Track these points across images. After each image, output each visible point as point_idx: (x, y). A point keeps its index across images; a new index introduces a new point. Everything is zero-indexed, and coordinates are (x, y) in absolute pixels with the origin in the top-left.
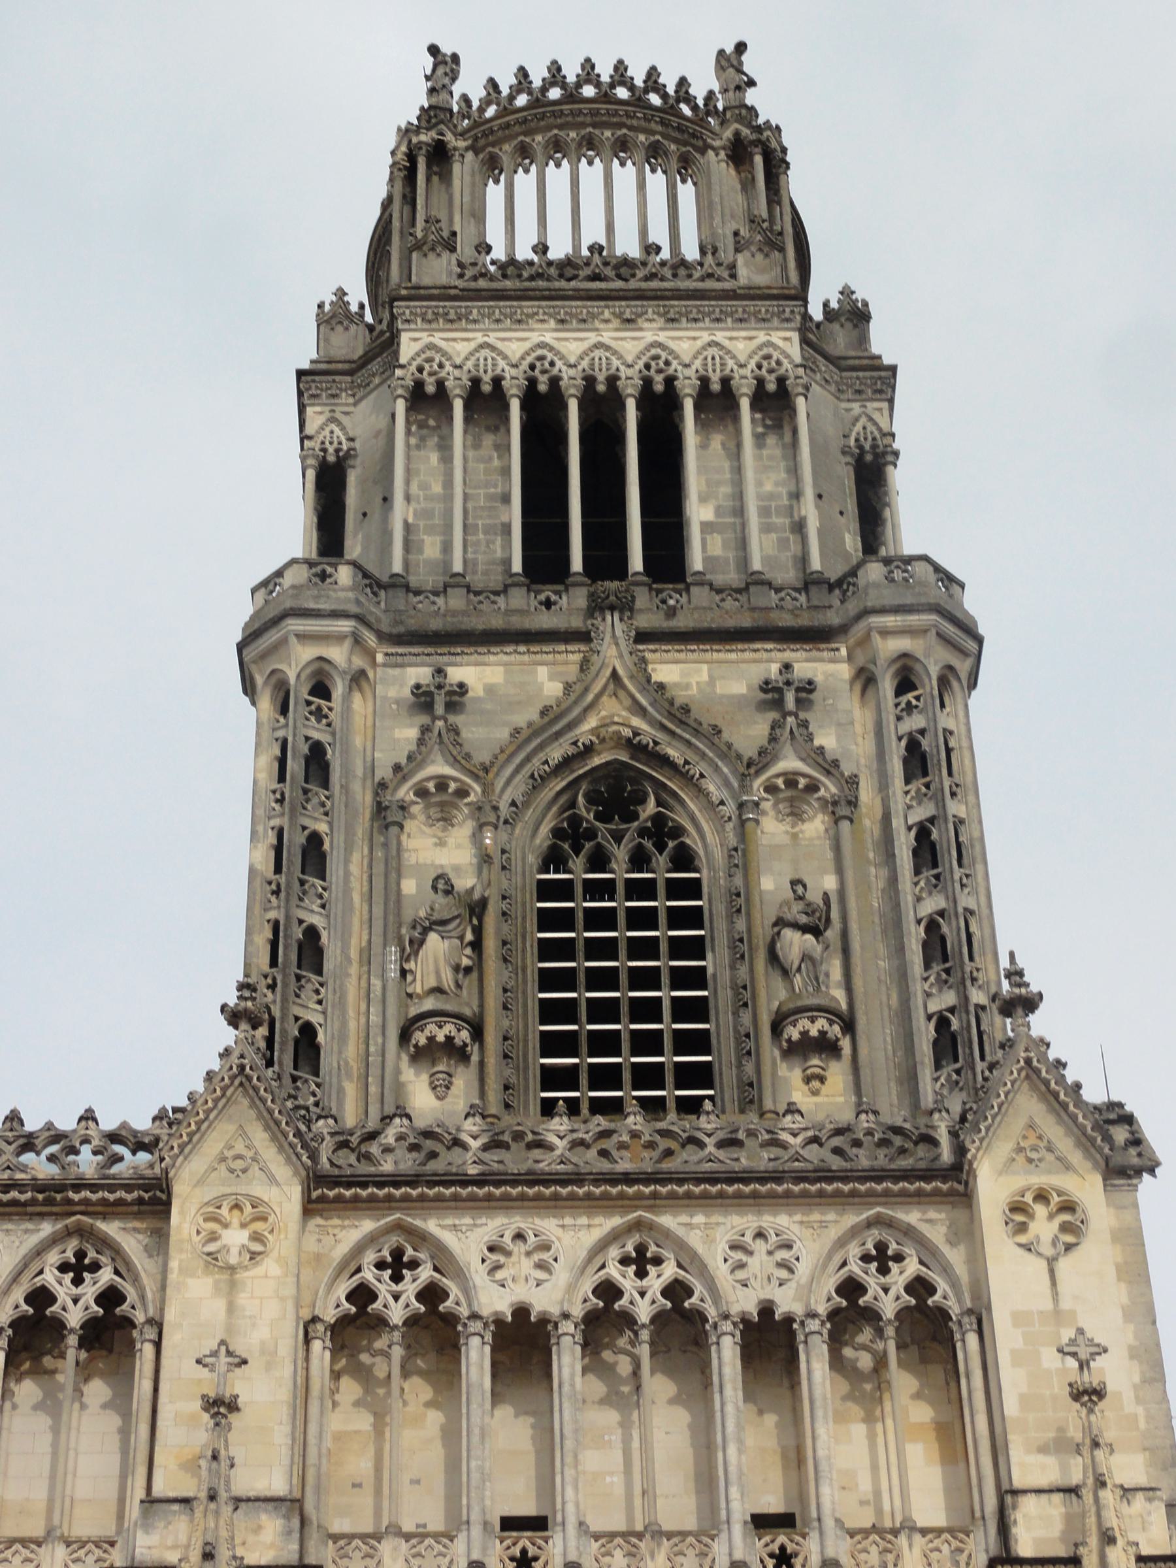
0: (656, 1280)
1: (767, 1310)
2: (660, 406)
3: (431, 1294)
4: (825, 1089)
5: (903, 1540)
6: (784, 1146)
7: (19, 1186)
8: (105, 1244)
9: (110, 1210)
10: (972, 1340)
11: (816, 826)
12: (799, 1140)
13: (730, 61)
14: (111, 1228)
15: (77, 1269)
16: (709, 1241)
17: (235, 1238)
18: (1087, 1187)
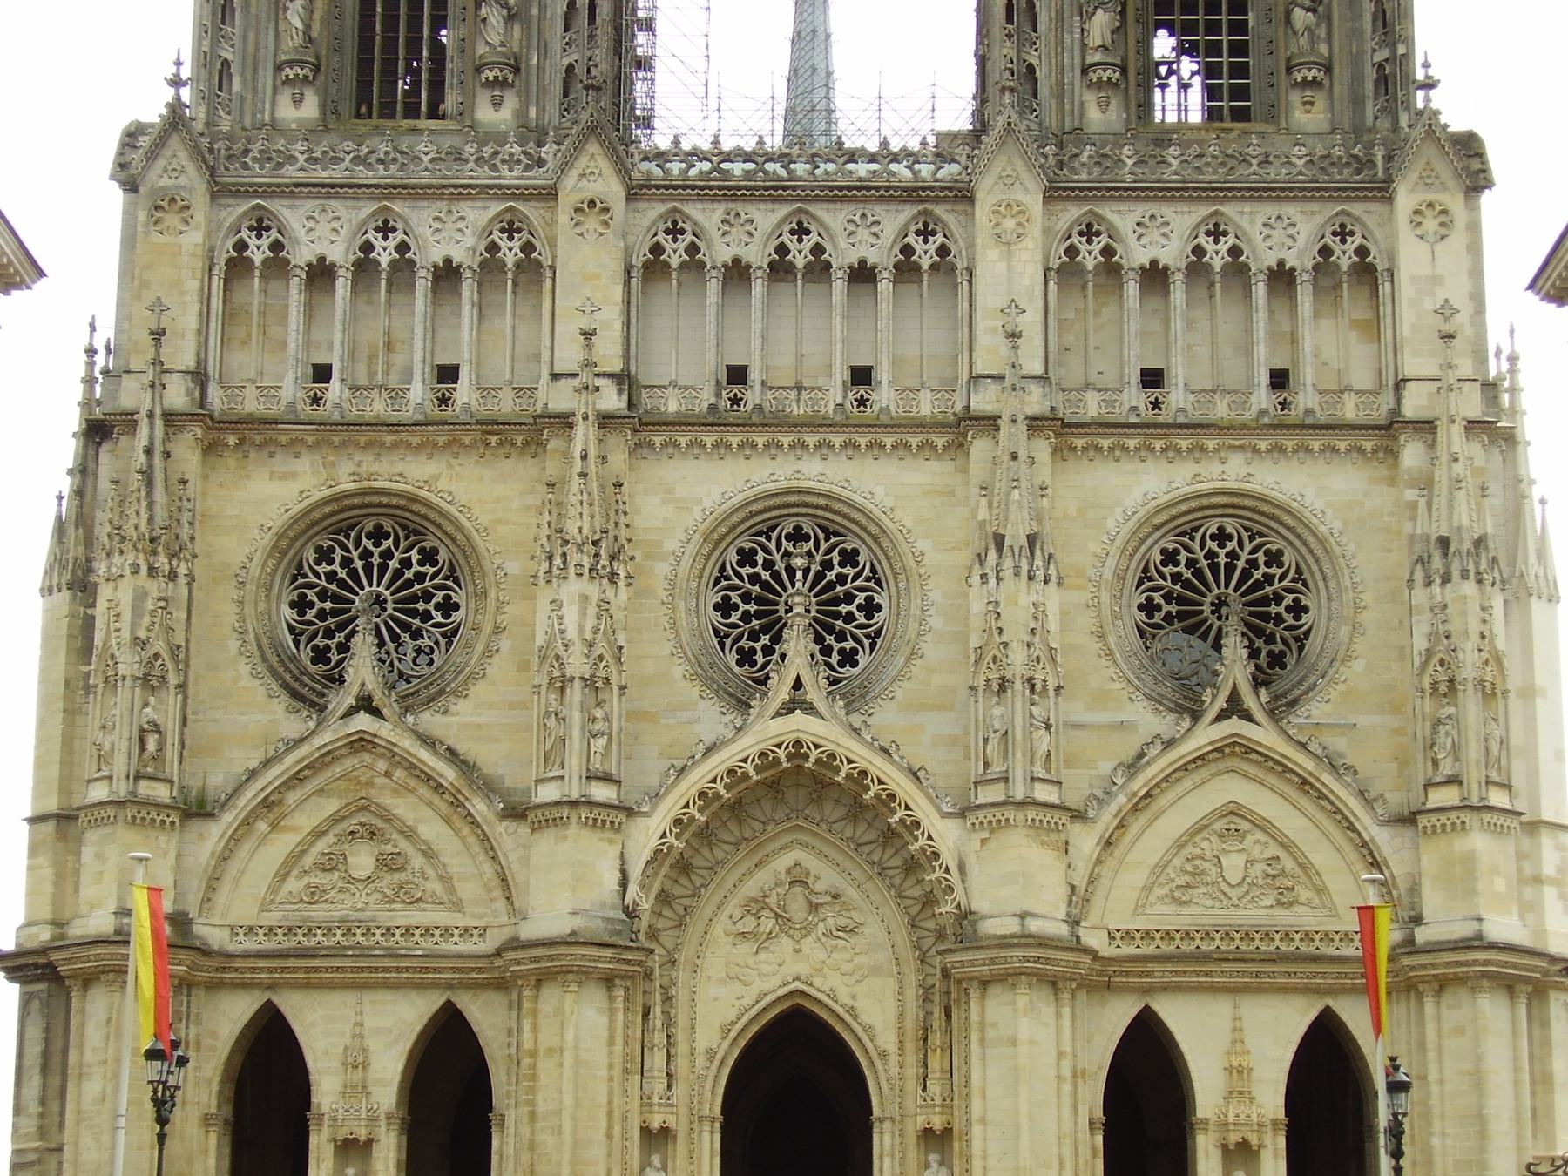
0: (1224, 246)
1: (1281, 264)
3: (1108, 252)
4: (1314, 109)
5: (1346, 395)
6: (1294, 165)
7: (896, 188)
8: (938, 221)
9: (937, 200)
10: (1387, 285)
12: (1303, 161)
14: (939, 210)
15: (925, 234)
16: (1252, 222)
17: (1009, 224)
18: (1454, 201)
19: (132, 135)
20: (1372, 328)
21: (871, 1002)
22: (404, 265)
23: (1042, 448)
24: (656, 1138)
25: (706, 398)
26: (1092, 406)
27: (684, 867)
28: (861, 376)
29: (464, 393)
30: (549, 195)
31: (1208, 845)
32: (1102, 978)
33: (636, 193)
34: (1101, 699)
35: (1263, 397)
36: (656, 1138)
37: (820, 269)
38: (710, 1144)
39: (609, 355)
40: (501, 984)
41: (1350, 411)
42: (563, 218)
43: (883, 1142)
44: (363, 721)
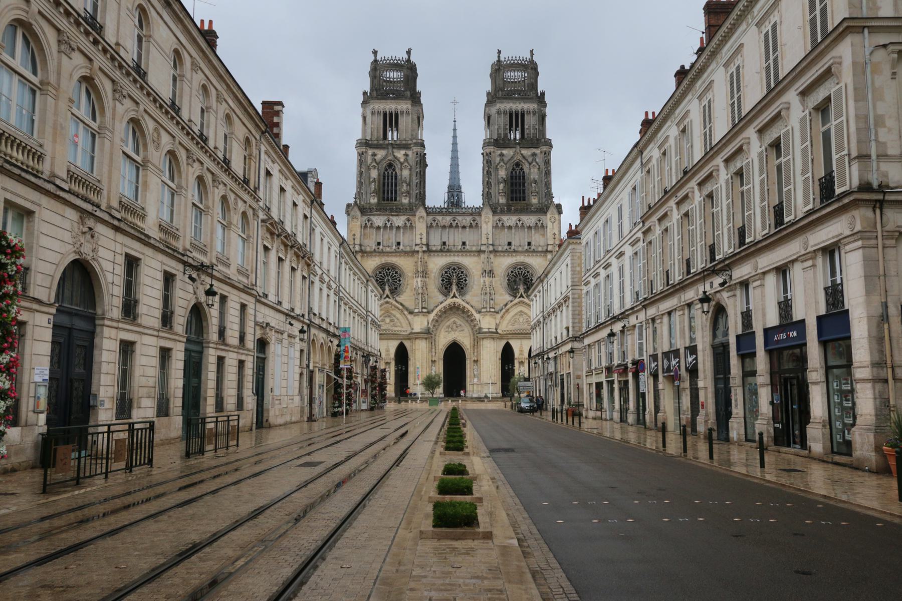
2: (523, 115)
11: (536, 170)
13: (532, 51)
18: (556, 216)
19: (349, 206)
20: (543, 235)
21: (466, 341)
22: (391, 227)
23: (492, 256)
24: (433, 362)
25: (439, 248)
26: (500, 249)
27: (437, 321)
28: (464, 243)
29: (401, 247)
30: (414, 215)
31: (517, 317)
32: (501, 337)
33: (428, 214)
34: (501, 295)
35: (526, 247)
36: (433, 362)
37: (457, 226)
38: (441, 363)
39: (424, 241)
40: (409, 339)
41: (540, 249)
42: (417, 219)
43: (468, 362)
44: (387, 299)
